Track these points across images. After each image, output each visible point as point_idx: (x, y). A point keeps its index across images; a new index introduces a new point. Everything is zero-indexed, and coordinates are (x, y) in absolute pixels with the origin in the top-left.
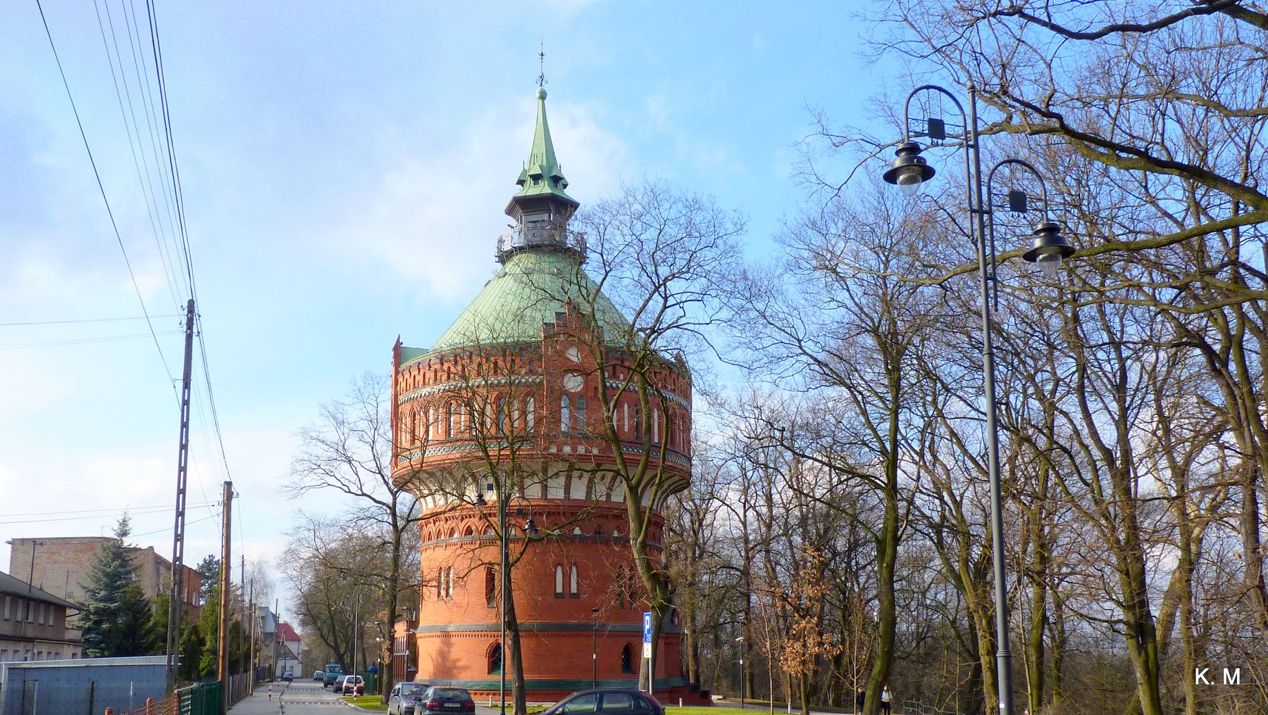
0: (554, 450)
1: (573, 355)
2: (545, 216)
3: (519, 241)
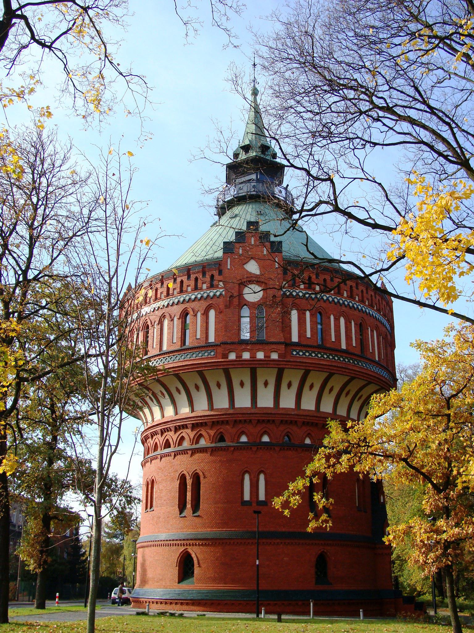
0: (232, 356)
1: (253, 267)
2: (254, 177)
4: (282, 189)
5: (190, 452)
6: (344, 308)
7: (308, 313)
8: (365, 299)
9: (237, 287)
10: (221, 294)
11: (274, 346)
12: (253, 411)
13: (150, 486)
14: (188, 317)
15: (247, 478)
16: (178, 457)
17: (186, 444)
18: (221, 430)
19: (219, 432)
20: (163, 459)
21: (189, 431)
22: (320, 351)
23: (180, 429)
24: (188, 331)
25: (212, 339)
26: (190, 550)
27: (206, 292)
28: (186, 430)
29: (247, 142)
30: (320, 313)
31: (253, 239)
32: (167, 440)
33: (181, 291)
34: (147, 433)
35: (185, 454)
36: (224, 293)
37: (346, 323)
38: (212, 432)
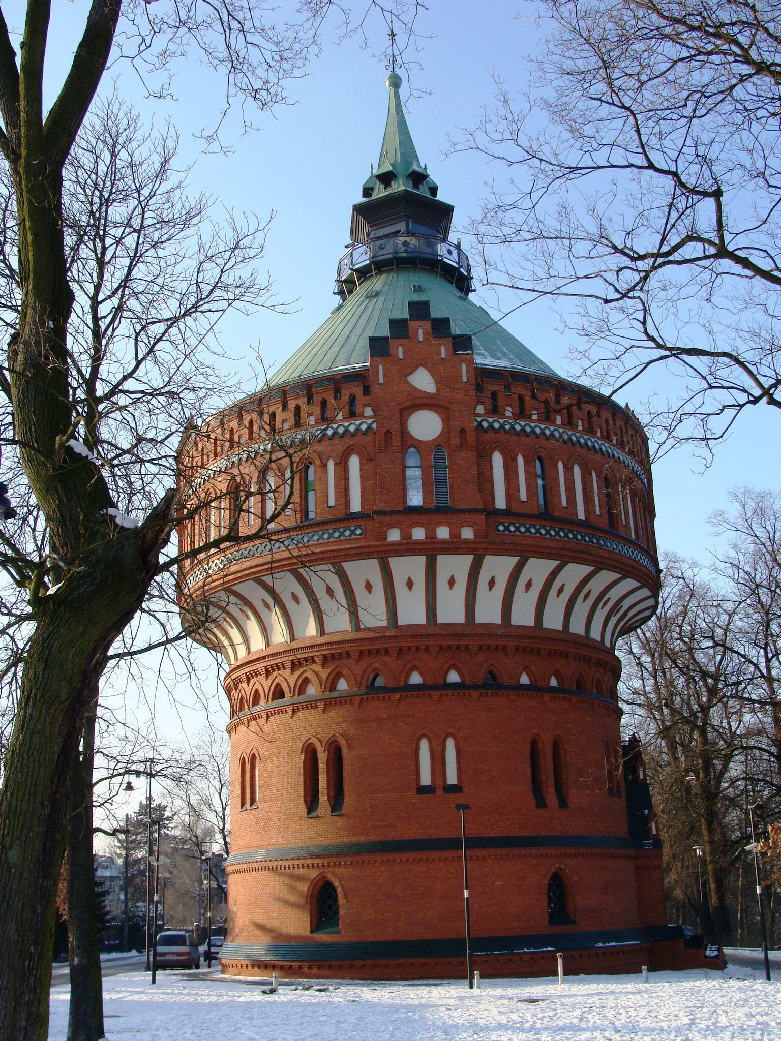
0: (394, 535)
1: (423, 381)
2: (402, 226)
3: (362, 257)
4: (452, 249)
5: (321, 705)
6: (579, 450)
7: (520, 460)
8: (612, 433)
9: (398, 415)
10: (369, 428)
11: (467, 517)
12: (431, 630)
13: (248, 766)
14: (311, 469)
15: (424, 745)
16: (301, 714)
17: (312, 690)
18: (376, 665)
19: (370, 669)
20: (271, 719)
21: (317, 668)
22: (544, 523)
23: (300, 664)
24: (311, 495)
25: (356, 506)
26: (330, 877)
27: (341, 424)
28: (313, 667)
29: (387, 168)
30: (540, 459)
31: (420, 332)
32: (278, 684)
33: (298, 424)
34: (238, 674)
35: (312, 707)
36: (374, 426)
37: (583, 475)
38: (358, 669)
